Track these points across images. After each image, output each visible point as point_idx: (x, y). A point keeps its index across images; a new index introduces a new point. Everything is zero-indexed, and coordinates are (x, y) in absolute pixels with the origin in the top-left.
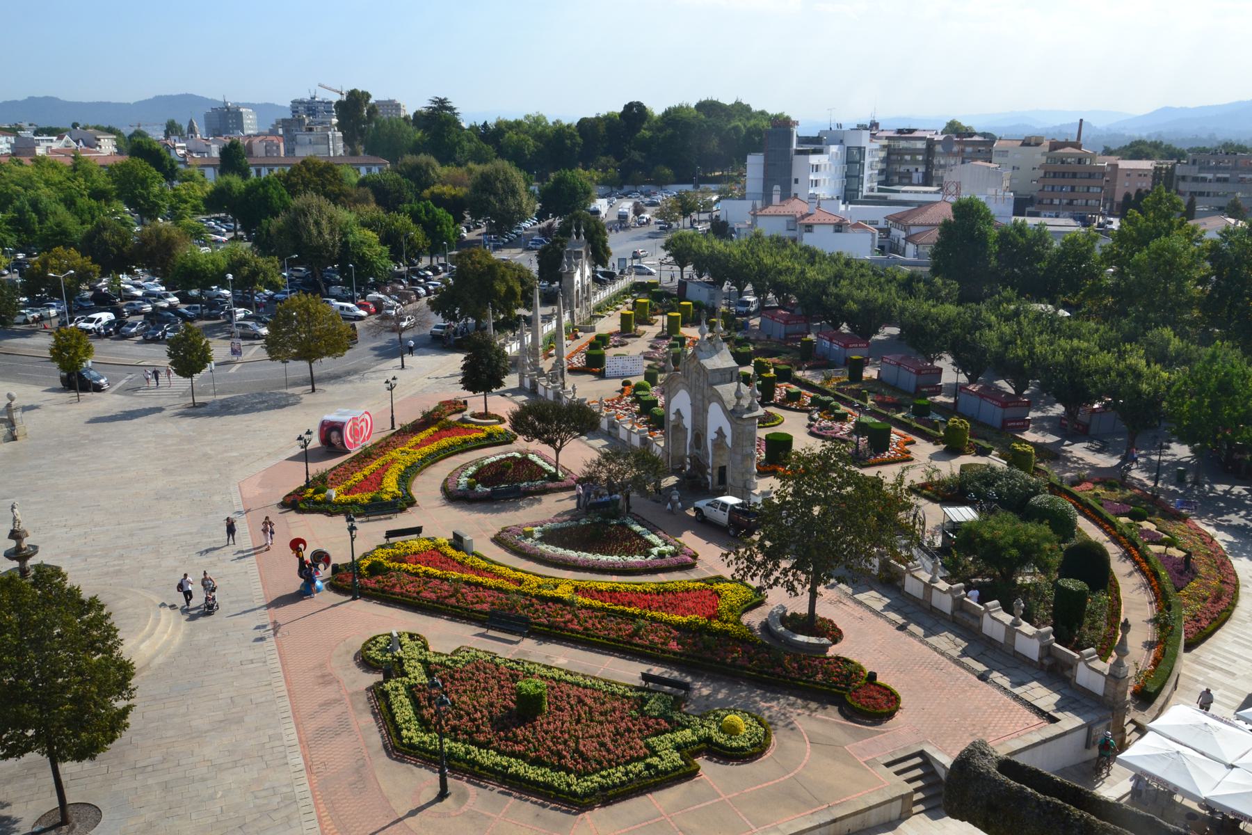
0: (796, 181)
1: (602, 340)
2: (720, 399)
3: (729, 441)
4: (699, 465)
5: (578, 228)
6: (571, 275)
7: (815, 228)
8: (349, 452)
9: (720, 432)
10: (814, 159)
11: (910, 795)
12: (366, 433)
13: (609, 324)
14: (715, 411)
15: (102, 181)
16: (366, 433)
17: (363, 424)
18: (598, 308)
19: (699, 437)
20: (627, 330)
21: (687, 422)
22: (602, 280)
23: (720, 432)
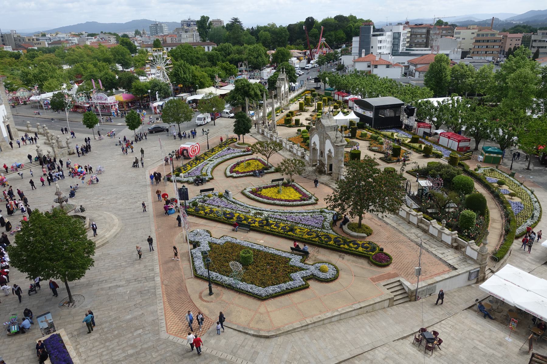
0: (372, 47)
1: (292, 113)
2: (330, 138)
3: (333, 154)
4: (323, 165)
5: (283, 69)
6: (280, 88)
7: (379, 66)
8: (191, 159)
9: (330, 151)
10: (379, 38)
11: (393, 298)
12: (197, 151)
13: (295, 107)
14: (328, 142)
15: (109, 55)
16: (197, 151)
17: (196, 148)
18: (291, 100)
19: (322, 153)
20: (301, 109)
21: (318, 147)
22: (292, 89)
23: (330, 151)
